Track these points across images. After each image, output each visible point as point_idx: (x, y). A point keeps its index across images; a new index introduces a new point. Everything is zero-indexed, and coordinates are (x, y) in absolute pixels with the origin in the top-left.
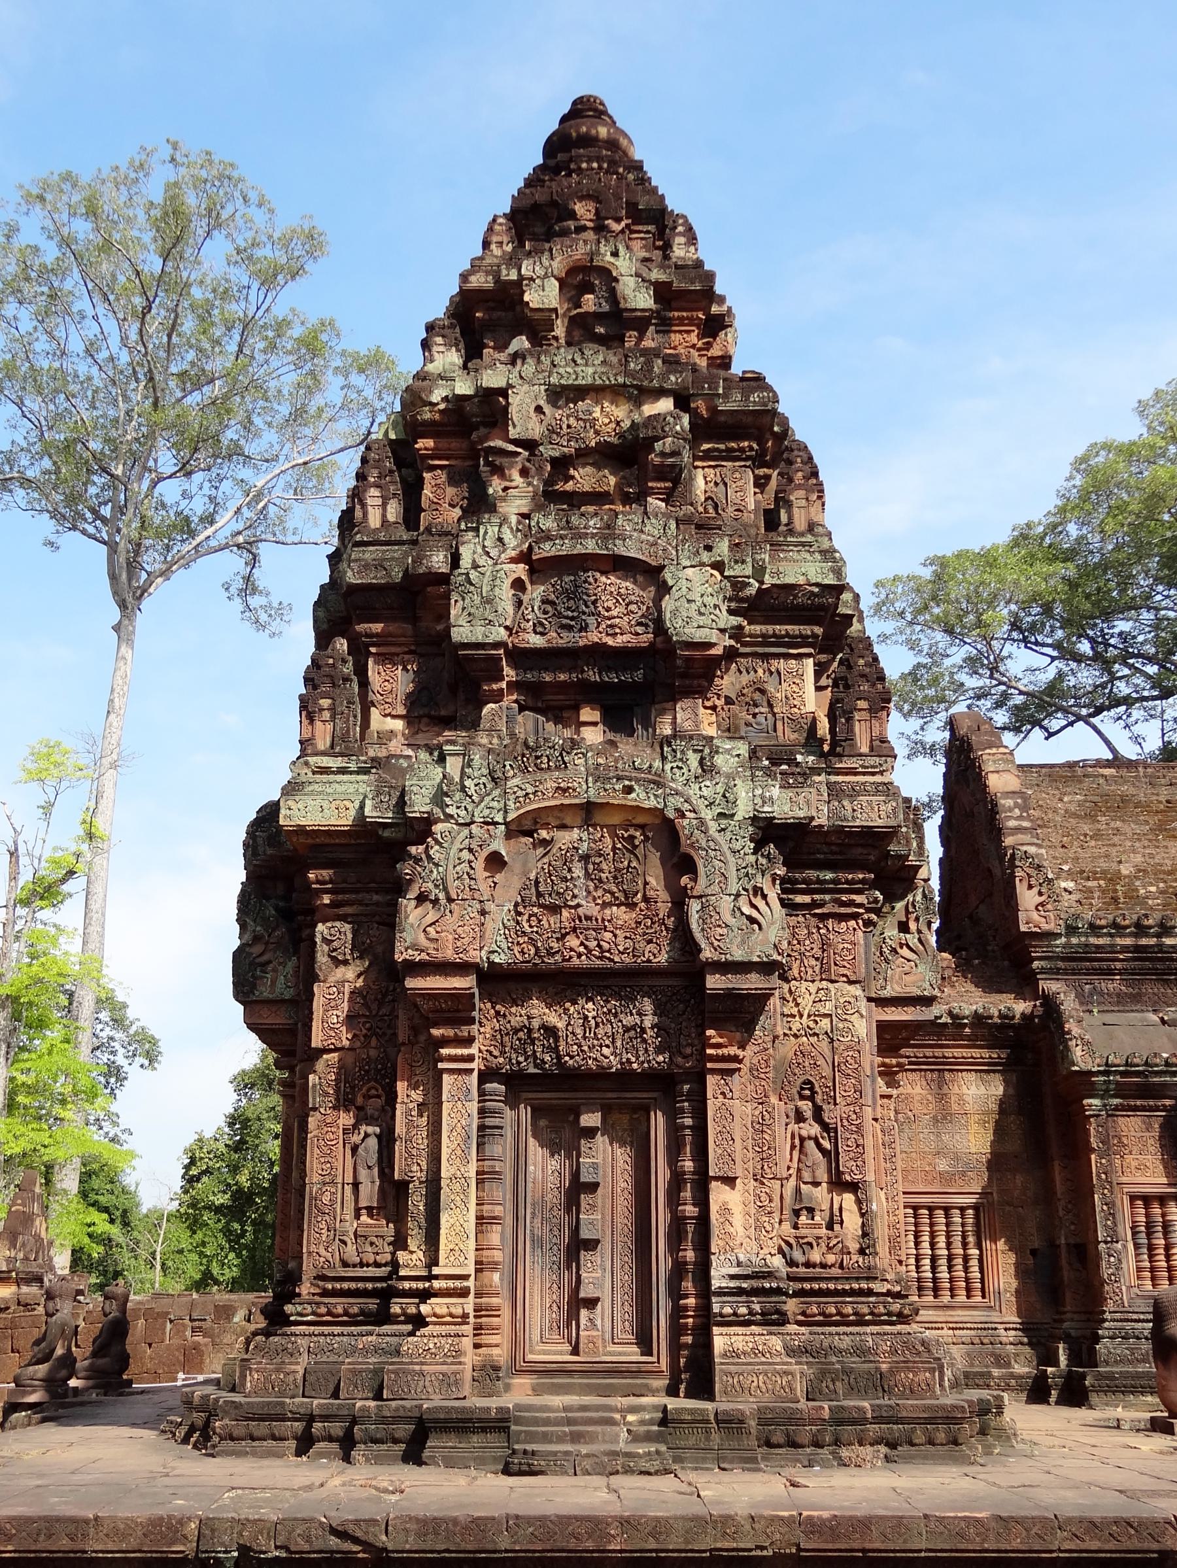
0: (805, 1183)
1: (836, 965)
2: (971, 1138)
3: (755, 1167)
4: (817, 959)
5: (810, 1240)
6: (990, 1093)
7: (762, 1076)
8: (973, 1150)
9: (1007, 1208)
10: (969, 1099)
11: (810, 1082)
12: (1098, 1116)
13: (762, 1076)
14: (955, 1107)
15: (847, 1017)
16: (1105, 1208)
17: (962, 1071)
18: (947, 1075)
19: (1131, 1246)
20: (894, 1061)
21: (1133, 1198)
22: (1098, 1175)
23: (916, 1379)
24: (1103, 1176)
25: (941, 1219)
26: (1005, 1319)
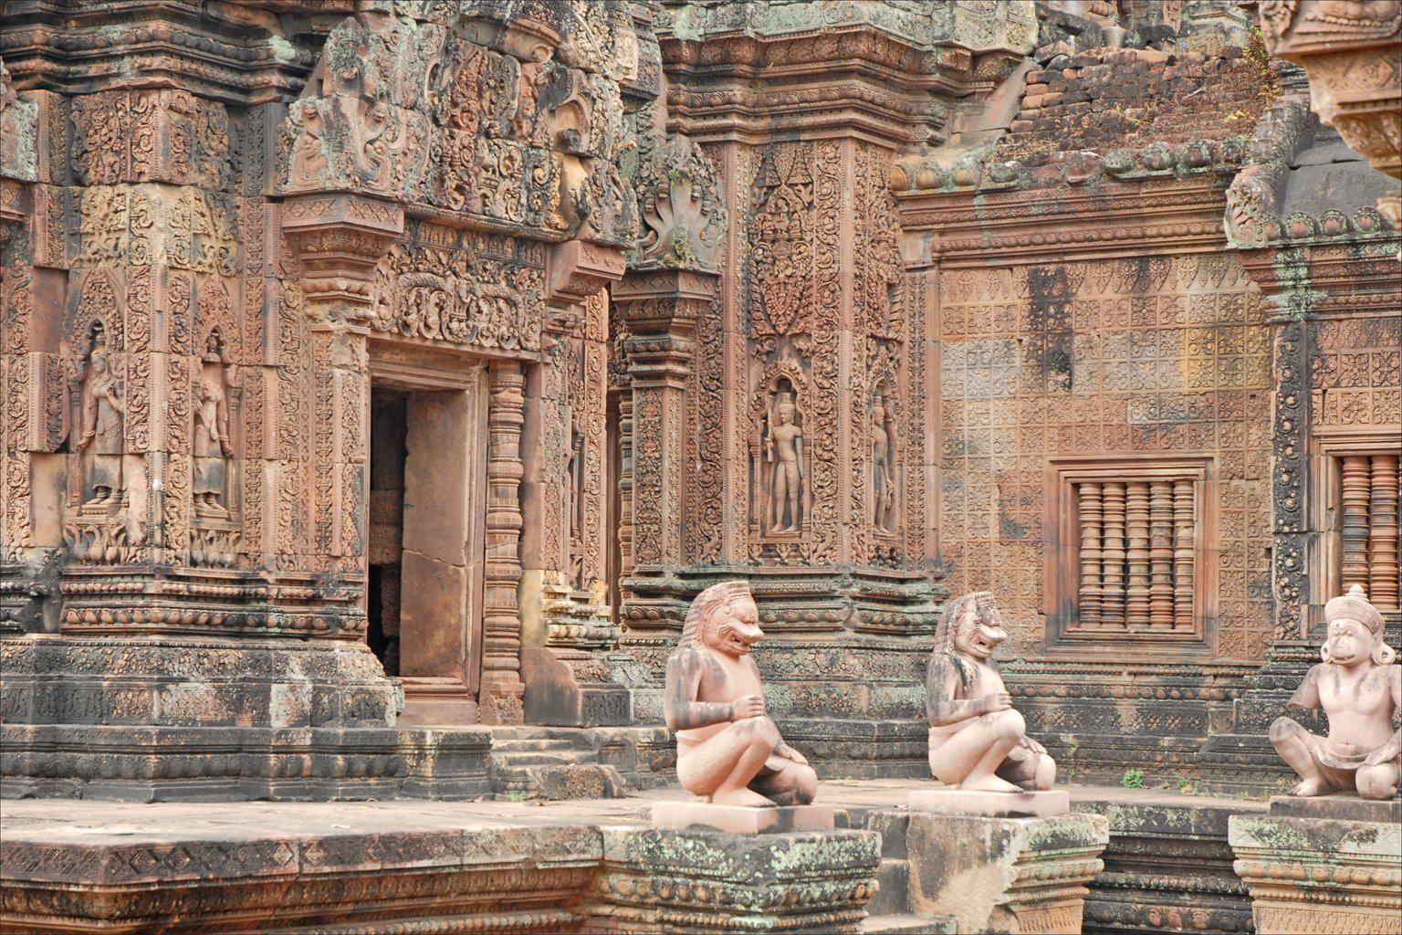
0: (100, 455)
1: (133, 159)
2: (1183, 366)
3: (9, 438)
4: (118, 153)
5: (90, 528)
6: (1219, 291)
7: (21, 319)
8: (1186, 389)
9: (1235, 482)
10: (1186, 303)
11: (100, 325)
12: (1287, 323)
13: (21, 319)
14: (1161, 319)
15: (142, 231)
16: (1285, 478)
17: (1177, 256)
18: (1154, 267)
19: (1328, 543)
20: (324, 283)
21: (1340, 461)
22: (1279, 424)
23: (135, 700)
24: (1287, 426)
25: (1137, 502)
26: (1218, 661)
